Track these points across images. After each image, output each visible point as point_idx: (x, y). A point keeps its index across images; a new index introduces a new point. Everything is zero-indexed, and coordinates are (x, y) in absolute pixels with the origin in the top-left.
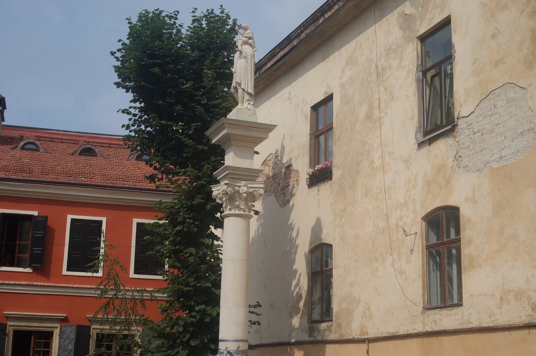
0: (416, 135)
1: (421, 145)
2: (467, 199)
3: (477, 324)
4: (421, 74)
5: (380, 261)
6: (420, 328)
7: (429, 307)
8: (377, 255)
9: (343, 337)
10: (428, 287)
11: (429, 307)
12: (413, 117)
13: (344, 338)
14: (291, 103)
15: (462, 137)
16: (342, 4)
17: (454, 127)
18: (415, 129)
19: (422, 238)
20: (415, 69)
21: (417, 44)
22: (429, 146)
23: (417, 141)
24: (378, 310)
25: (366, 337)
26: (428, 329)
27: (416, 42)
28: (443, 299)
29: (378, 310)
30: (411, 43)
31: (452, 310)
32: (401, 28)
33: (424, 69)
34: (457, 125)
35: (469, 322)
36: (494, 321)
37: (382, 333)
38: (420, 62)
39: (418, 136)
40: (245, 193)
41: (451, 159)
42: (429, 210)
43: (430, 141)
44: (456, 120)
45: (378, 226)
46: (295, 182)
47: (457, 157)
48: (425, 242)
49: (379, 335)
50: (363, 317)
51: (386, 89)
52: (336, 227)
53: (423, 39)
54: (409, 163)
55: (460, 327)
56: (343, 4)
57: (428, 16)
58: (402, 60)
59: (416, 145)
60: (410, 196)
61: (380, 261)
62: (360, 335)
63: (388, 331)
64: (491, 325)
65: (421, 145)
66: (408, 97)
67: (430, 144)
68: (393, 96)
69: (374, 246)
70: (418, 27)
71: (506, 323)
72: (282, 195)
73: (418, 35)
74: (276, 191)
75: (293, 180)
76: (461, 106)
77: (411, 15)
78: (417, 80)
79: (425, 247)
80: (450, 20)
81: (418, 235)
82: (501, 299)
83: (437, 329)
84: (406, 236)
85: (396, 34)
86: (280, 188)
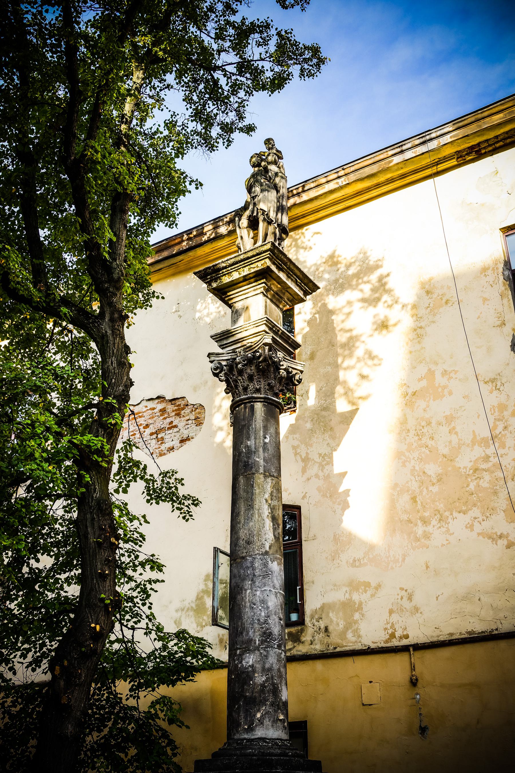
5: (434, 522)
8: (427, 514)
9: (335, 648)
13: (338, 650)
14: (180, 317)
16: (344, 183)
24: (437, 598)
25: (405, 642)
29: (437, 598)
37: (451, 634)
45: (424, 472)
46: (190, 422)
50: (391, 612)
52: (308, 479)
54: (499, 384)
56: (347, 182)
61: (434, 522)
62: (386, 642)
63: (469, 630)
66: (485, 300)
68: (447, 300)
69: (415, 502)
75: (187, 418)
86: (148, 431)
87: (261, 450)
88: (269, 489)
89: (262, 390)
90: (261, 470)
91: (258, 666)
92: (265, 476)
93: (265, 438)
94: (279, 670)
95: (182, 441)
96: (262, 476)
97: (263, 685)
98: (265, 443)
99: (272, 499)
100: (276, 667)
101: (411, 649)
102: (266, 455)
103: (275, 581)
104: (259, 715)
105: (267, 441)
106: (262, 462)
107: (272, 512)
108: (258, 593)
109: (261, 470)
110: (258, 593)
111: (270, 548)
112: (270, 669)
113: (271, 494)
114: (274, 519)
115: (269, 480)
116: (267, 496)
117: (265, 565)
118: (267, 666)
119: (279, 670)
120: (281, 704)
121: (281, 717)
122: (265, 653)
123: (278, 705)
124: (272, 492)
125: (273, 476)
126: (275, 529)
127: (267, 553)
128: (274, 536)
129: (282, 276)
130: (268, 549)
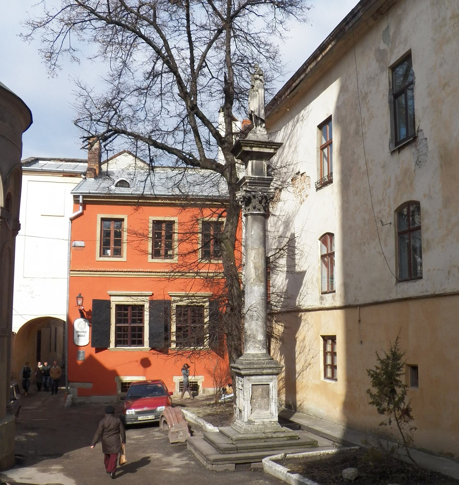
0: (389, 145)
1: (393, 152)
2: (425, 195)
3: (433, 292)
4: (392, 97)
6: (394, 296)
7: (400, 280)
10: (399, 265)
11: (400, 280)
12: (387, 132)
15: (421, 146)
17: (415, 138)
18: (388, 141)
19: (395, 226)
20: (388, 93)
21: (389, 73)
22: (398, 153)
23: (390, 150)
26: (399, 296)
27: (387, 72)
28: (410, 274)
30: (384, 73)
31: (415, 282)
32: (378, 61)
33: (394, 93)
34: (417, 136)
35: (427, 291)
36: (443, 290)
38: (391, 87)
39: (391, 146)
40: (260, 197)
41: (414, 164)
42: (399, 205)
43: (400, 150)
44: (416, 132)
47: (418, 162)
48: (397, 229)
49: (367, 302)
51: (368, 110)
53: (393, 68)
55: (421, 295)
57: (396, 51)
58: (378, 86)
59: (390, 153)
60: (386, 194)
64: (442, 292)
65: (393, 152)
67: (399, 152)
70: (389, 59)
71: (452, 291)
72: (299, 196)
73: (389, 65)
74: (295, 193)
76: (420, 121)
77: (384, 50)
78: (390, 102)
79: (397, 234)
80: (411, 54)
81: (392, 224)
82: (449, 272)
83: (405, 296)
84: (383, 225)
85: (375, 65)
87: (250, 238)
88: (253, 255)
89: (250, 209)
90: (250, 248)
91: (248, 328)
92: (252, 250)
93: (252, 232)
94: (256, 329)
95: (306, 196)
96: (250, 250)
97: (250, 335)
98: (252, 235)
99: (254, 260)
100: (254, 328)
101: (358, 307)
102: (252, 240)
103: (256, 294)
104: (248, 346)
105: (252, 233)
106: (250, 243)
107: (255, 265)
108: (249, 300)
109: (250, 248)
110: (249, 300)
111: (253, 281)
112: (252, 329)
113: (254, 257)
114: (255, 268)
115: (253, 251)
116: (252, 259)
117: (251, 288)
118: (251, 328)
119: (256, 329)
120: (257, 341)
121: (258, 346)
122: (250, 323)
123: (256, 342)
124: (255, 256)
125: (256, 249)
126: (256, 272)
127: (252, 283)
128: (255, 275)
129: (255, 149)
130: (252, 281)
